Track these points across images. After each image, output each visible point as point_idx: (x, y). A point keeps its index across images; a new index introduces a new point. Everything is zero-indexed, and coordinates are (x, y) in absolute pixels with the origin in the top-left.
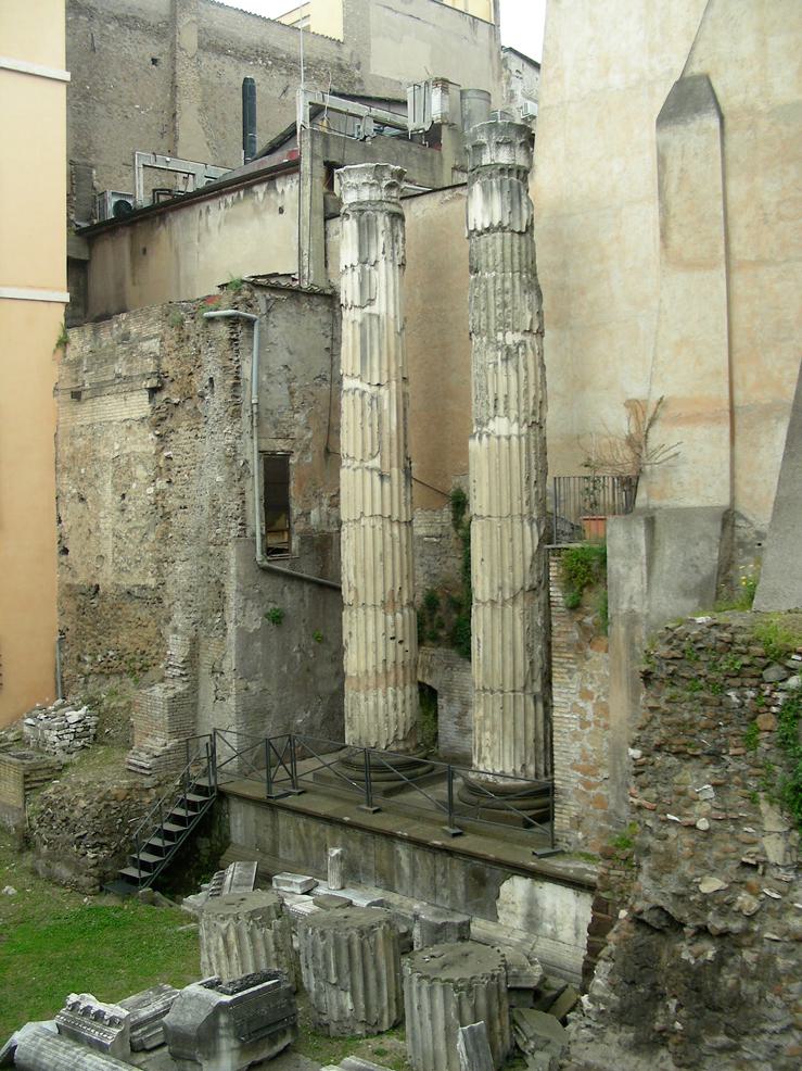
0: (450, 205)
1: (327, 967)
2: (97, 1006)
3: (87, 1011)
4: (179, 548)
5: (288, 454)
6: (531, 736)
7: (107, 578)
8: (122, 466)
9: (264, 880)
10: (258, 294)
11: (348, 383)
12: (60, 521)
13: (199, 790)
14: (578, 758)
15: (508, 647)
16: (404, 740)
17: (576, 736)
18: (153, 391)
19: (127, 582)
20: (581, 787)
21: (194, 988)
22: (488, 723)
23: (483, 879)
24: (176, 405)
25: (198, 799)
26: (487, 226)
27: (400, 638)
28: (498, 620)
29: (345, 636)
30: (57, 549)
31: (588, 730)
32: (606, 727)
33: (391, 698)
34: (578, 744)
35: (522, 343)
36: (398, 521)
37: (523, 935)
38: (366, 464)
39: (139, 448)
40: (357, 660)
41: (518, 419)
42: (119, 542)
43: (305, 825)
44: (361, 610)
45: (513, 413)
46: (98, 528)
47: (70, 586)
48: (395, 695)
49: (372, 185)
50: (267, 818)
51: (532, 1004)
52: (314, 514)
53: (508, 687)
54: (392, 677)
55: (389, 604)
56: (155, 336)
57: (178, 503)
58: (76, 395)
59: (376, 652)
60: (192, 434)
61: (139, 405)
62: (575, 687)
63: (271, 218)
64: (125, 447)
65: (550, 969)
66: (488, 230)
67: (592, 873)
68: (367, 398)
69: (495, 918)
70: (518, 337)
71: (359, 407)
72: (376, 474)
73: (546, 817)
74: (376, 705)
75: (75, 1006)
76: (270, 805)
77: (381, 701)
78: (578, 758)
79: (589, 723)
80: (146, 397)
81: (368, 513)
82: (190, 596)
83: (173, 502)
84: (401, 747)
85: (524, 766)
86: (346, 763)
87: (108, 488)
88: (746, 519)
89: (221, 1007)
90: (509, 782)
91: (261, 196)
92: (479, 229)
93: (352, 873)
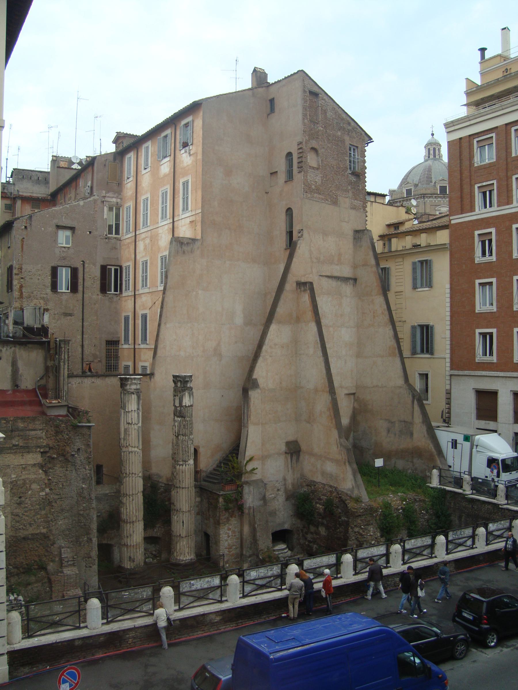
4: (59, 515)
17: (227, 540)
19: (22, 534)
24: (54, 458)
39: (32, 476)
42: (17, 518)
60: (64, 469)
62: (226, 528)
64: (21, 476)
66: (189, 406)
80: (39, 455)
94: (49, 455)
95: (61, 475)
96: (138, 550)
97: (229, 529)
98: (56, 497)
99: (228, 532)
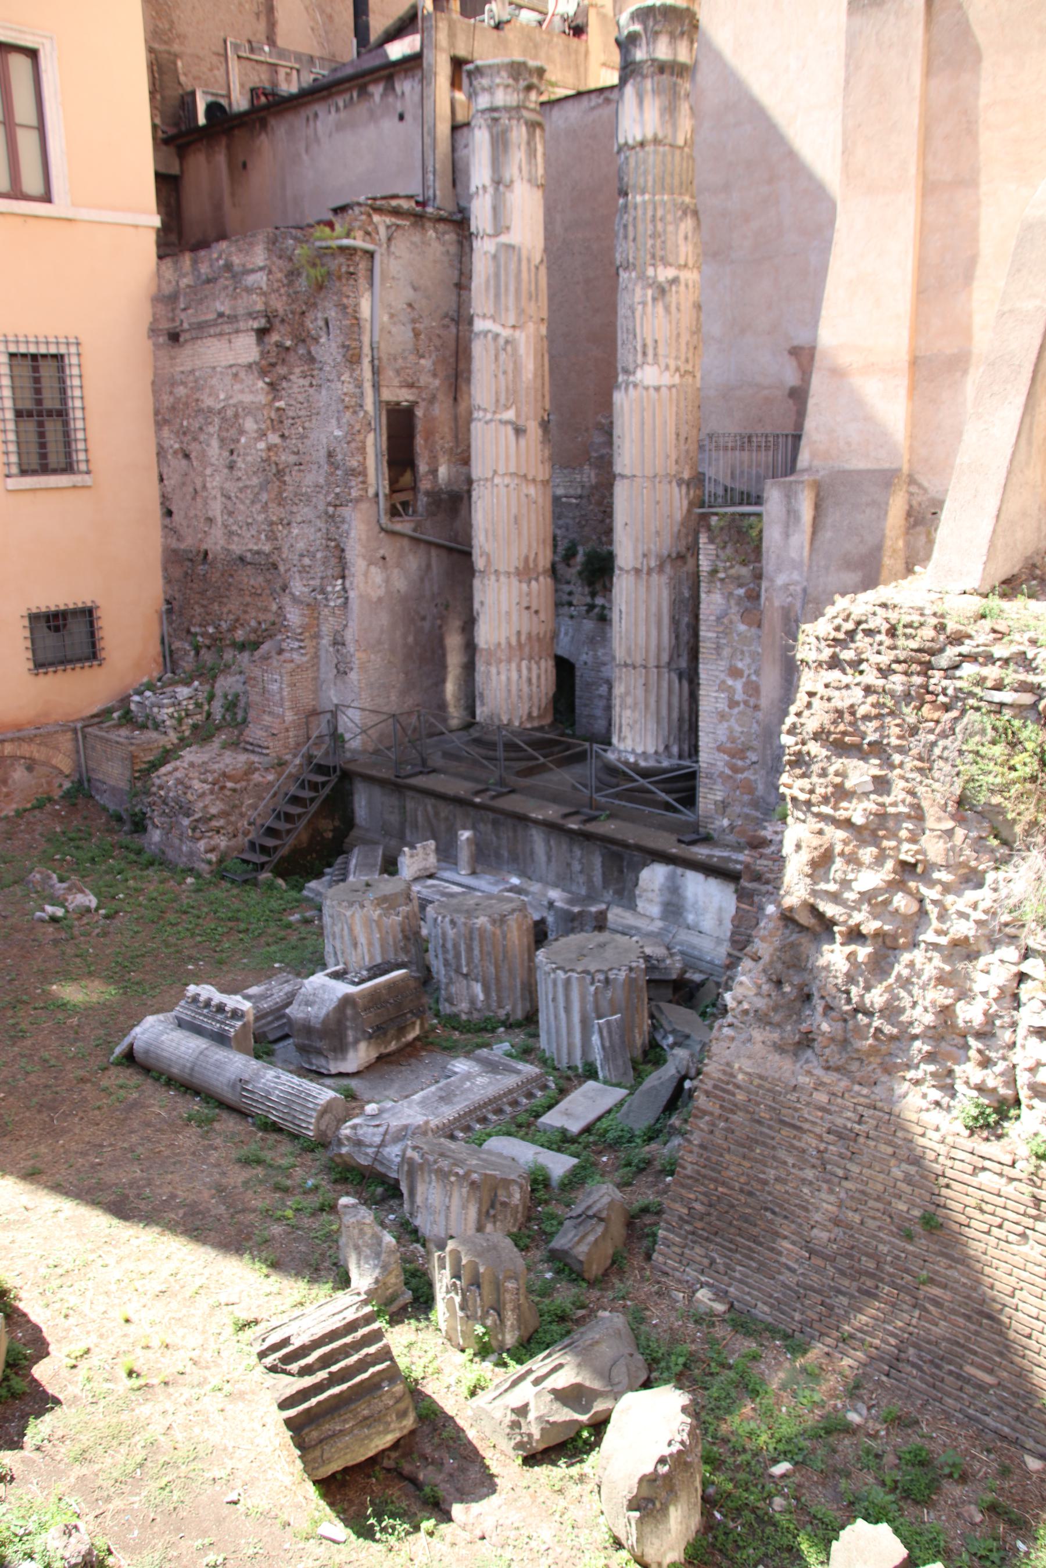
0: (596, 113)
1: (457, 956)
2: (218, 997)
3: (208, 1004)
4: (295, 509)
5: (415, 404)
6: (675, 715)
7: (215, 541)
8: (231, 421)
9: (390, 867)
10: (376, 218)
11: (479, 325)
12: (161, 480)
13: (321, 769)
14: (724, 739)
15: (653, 620)
16: (540, 717)
17: (722, 716)
18: (262, 333)
19: (236, 548)
20: (728, 771)
21: (319, 979)
22: (629, 700)
23: (622, 862)
24: (288, 349)
25: (321, 779)
26: (639, 138)
27: (534, 608)
28: (642, 590)
29: (476, 606)
30: (157, 511)
31: (736, 710)
32: (756, 707)
33: (525, 672)
34: (725, 725)
35: (675, 281)
36: (534, 480)
37: (659, 924)
38: (498, 416)
39: (247, 398)
40: (490, 632)
41: (667, 367)
43: (434, 806)
44: (493, 578)
45: (662, 361)
46: (204, 487)
47: (175, 551)
48: (529, 669)
49: (507, 86)
50: (394, 800)
51: (670, 996)
52: (443, 471)
53: (652, 662)
54: (527, 650)
55: (525, 573)
56: (261, 269)
57: (293, 459)
58: (174, 337)
59: (509, 622)
60: (306, 382)
61: (245, 348)
62: (723, 664)
63: (389, 124)
65: (691, 961)
66: (642, 144)
67: (737, 862)
68: (501, 341)
69: (632, 906)
70: (671, 273)
71: (492, 353)
72: (509, 428)
73: (690, 800)
74: (509, 679)
75: (195, 999)
76: (396, 787)
77: (514, 675)
78: (724, 739)
79: (737, 704)
80: (251, 339)
81: (501, 471)
82: (307, 561)
83: (286, 458)
84: (536, 724)
85: (667, 747)
86: (478, 742)
87: (215, 443)
88: (920, 486)
89: (347, 1001)
90: (651, 763)
91: (377, 98)
92: (630, 142)
93: (484, 858)
94: (275, 337)
95: (301, 398)
96: (493, 670)
97: (735, 673)
98: (293, 459)
99: (730, 682)
